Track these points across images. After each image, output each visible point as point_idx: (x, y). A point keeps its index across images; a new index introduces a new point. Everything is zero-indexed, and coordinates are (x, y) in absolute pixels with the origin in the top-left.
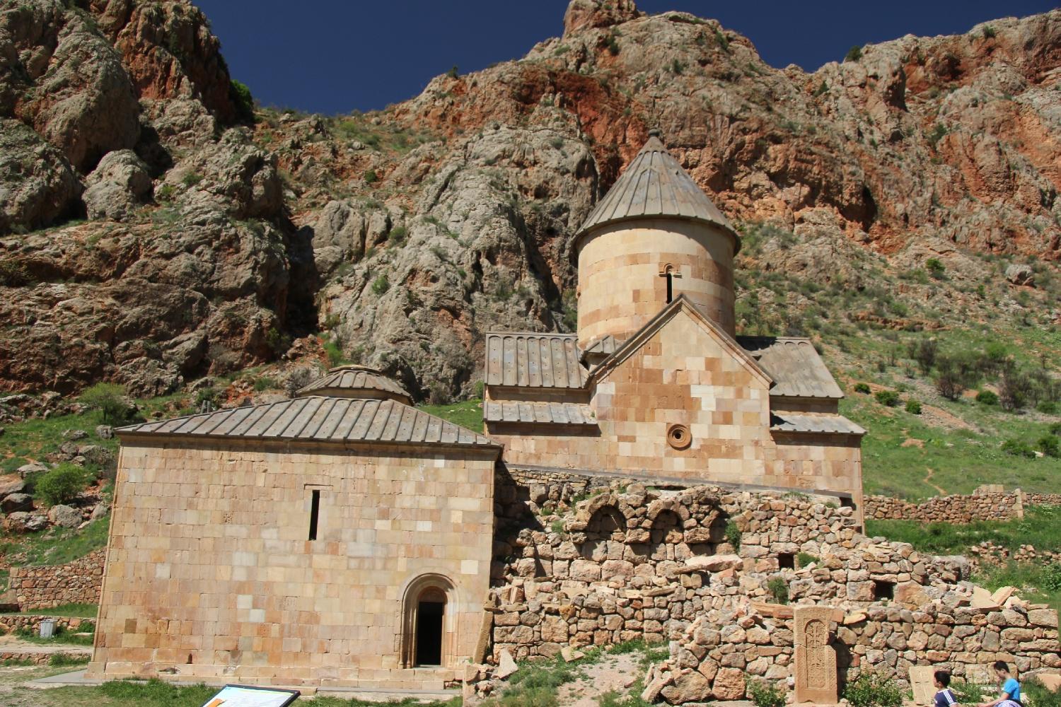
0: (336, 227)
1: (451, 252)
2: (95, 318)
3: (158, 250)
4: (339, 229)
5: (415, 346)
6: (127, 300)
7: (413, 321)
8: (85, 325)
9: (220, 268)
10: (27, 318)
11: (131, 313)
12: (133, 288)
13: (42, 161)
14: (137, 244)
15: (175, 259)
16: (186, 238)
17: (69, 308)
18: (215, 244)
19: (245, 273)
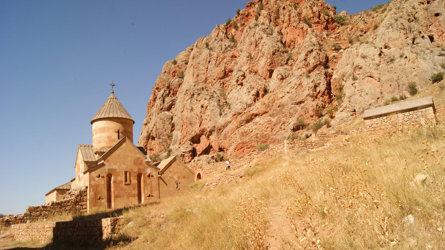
0: (347, 59)
1: (370, 53)
2: (266, 124)
3: (279, 97)
4: (349, 58)
5: (357, 97)
6: (274, 115)
7: (355, 87)
8: (263, 128)
9: (299, 94)
10: (251, 131)
11: (274, 120)
12: (275, 112)
13: (255, 83)
14: (274, 98)
15: (283, 98)
16: (288, 89)
17: (260, 124)
18: (296, 87)
19: (306, 93)
